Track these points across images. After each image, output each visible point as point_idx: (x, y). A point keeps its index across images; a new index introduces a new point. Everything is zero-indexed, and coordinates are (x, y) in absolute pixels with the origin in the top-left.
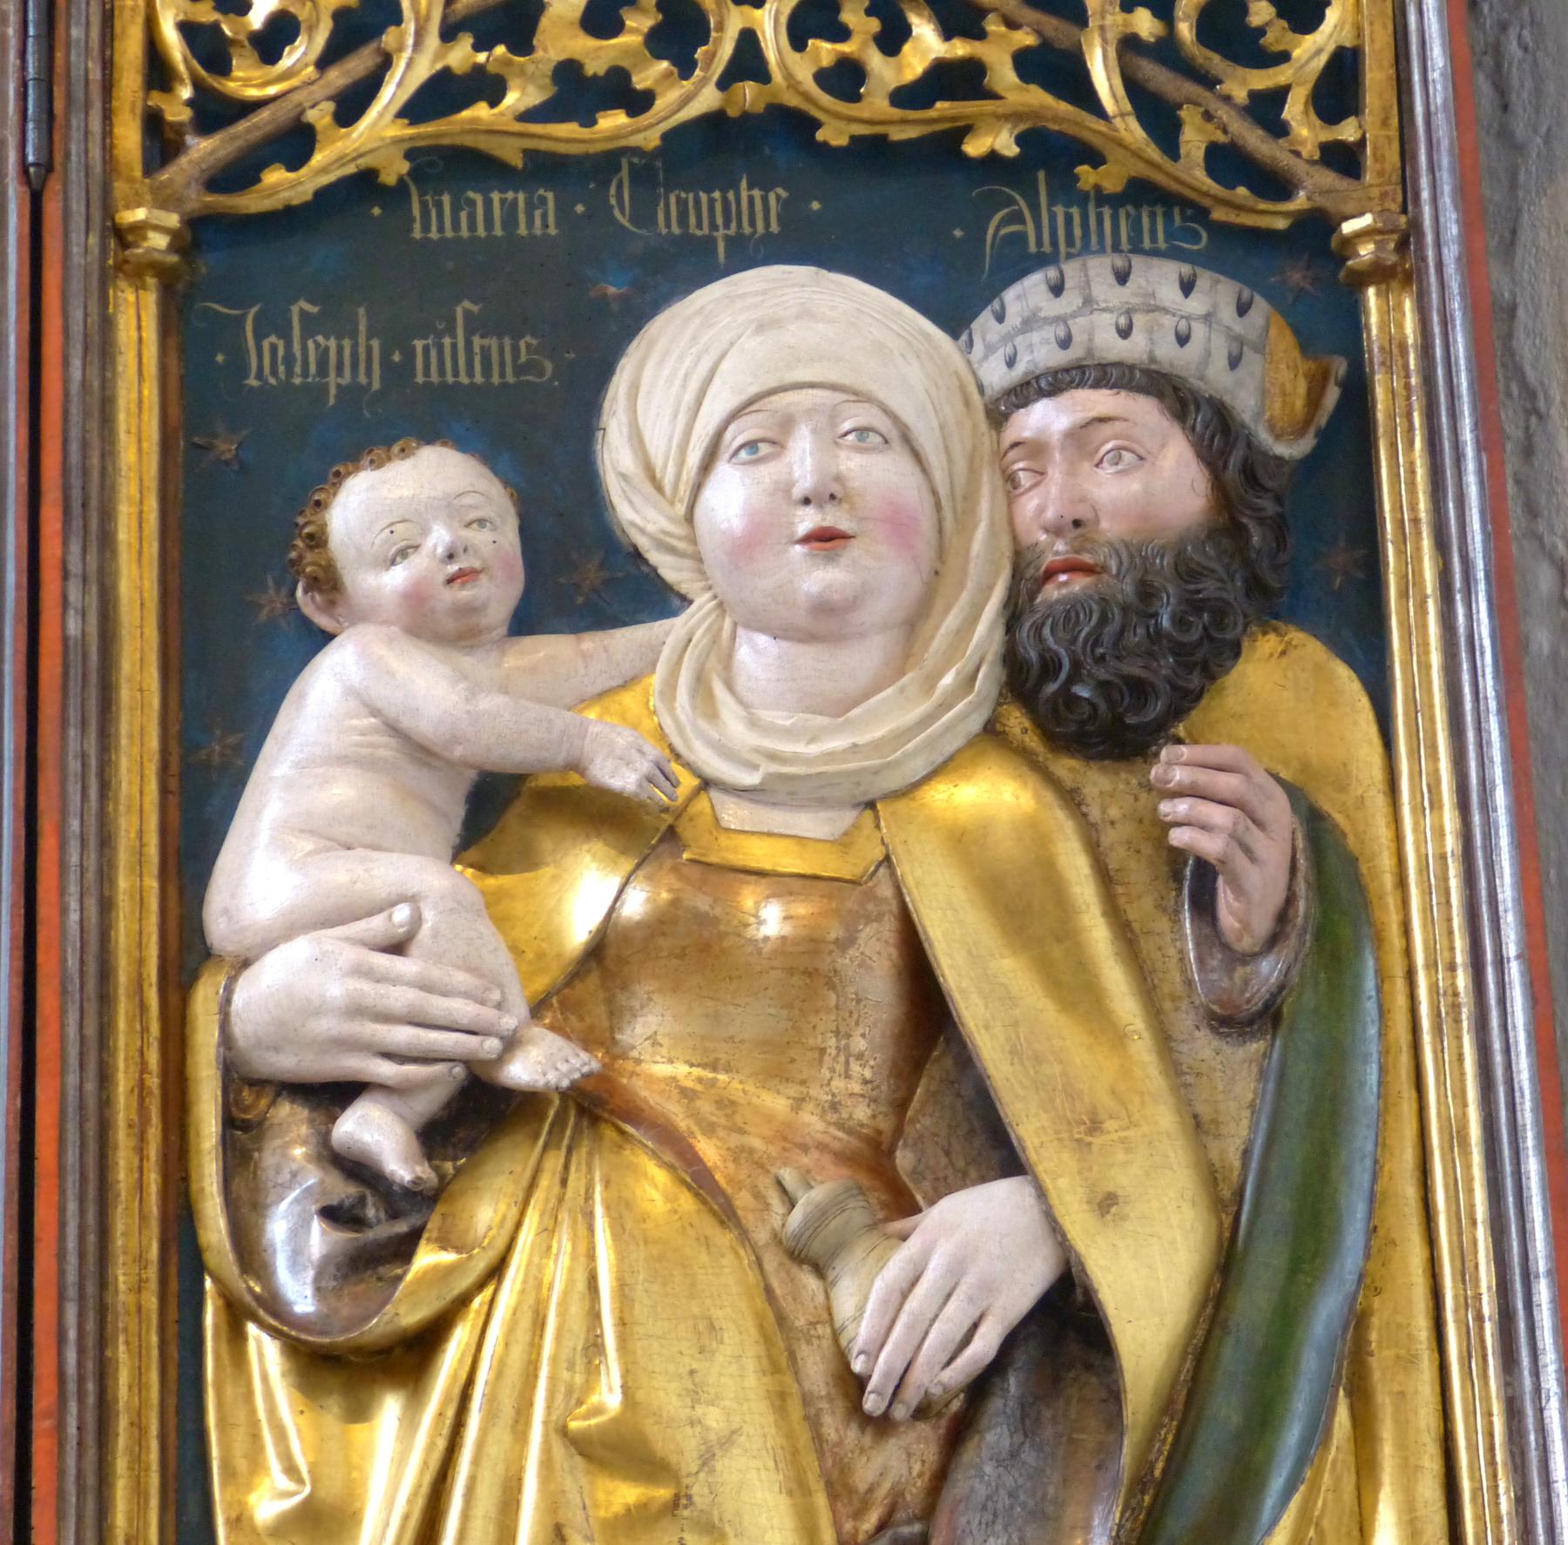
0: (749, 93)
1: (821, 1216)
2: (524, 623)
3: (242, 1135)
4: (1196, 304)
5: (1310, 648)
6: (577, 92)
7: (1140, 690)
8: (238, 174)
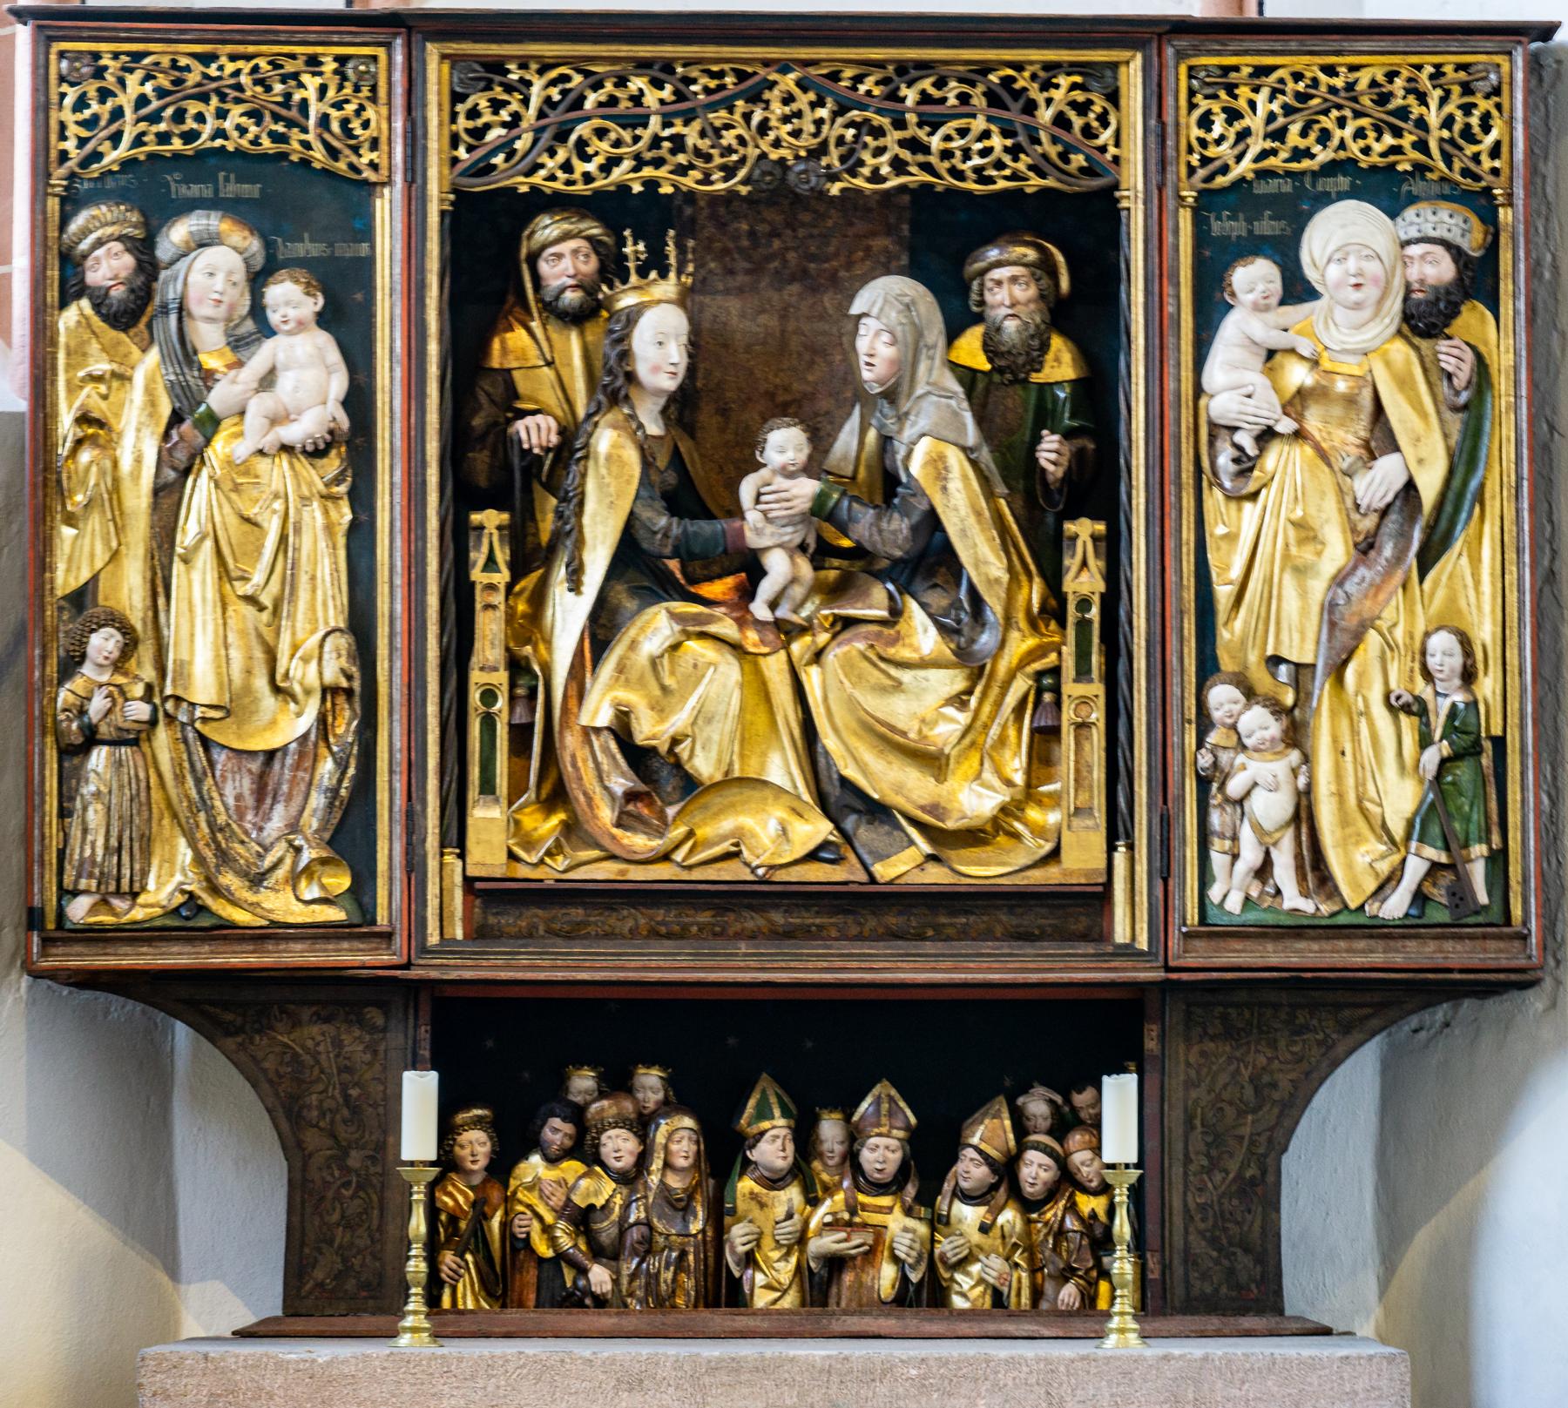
0: (1342, 155)
1: (1351, 465)
2: (1282, 303)
3: (1212, 438)
4: (1453, 221)
5: (1481, 307)
6: (1299, 154)
7: (1434, 325)
8: (1209, 178)
